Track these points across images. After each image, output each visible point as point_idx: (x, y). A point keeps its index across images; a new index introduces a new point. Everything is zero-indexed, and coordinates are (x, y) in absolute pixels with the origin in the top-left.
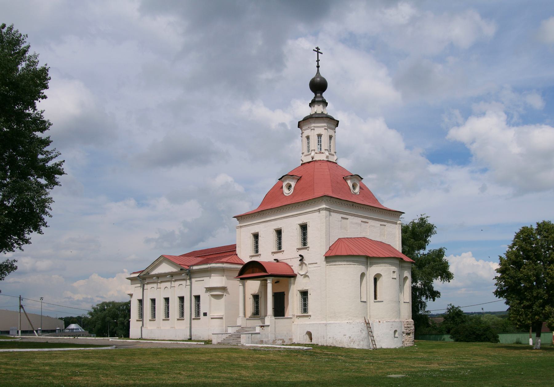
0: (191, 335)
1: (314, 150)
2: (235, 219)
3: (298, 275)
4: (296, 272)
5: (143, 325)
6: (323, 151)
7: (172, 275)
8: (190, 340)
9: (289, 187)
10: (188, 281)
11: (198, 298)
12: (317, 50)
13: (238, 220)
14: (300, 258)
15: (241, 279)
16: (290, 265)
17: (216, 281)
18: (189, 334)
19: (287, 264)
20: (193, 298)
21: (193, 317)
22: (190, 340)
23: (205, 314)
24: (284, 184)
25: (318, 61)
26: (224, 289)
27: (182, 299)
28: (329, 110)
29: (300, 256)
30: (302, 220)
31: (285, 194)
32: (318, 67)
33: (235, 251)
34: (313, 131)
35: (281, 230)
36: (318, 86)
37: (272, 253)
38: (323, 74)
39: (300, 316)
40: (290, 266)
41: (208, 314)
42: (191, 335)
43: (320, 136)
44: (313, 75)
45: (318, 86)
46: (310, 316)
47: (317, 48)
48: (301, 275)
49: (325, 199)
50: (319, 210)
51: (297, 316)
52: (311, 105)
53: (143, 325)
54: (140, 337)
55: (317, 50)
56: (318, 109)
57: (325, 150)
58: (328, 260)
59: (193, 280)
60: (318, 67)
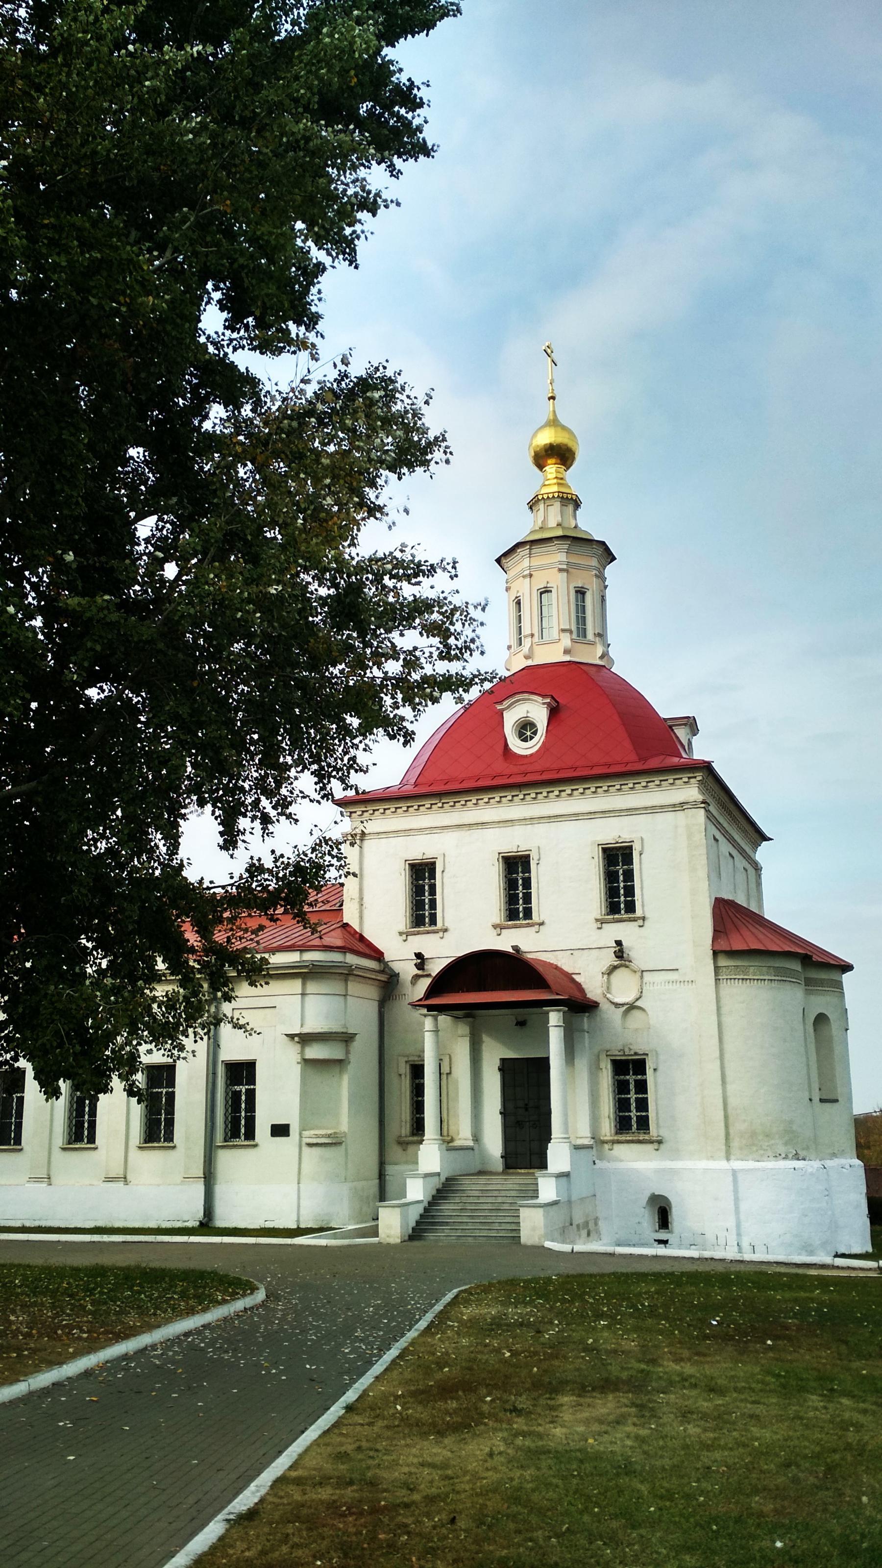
0: (209, 1210)
3: (604, 1006)
6: (590, 636)
9: (526, 729)
11: (242, 1072)
15: (430, 1008)
19: (557, 968)
20: (221, 1071)
22: (206, 1226)
23: (280, 1130)
24: (511, 718)
26: (346, 1038)
30: (613, 831)
33: (340, 910)
37: (495, 927)
42: (209, 1210)
43: (581, 593)
48: (617, 1005)
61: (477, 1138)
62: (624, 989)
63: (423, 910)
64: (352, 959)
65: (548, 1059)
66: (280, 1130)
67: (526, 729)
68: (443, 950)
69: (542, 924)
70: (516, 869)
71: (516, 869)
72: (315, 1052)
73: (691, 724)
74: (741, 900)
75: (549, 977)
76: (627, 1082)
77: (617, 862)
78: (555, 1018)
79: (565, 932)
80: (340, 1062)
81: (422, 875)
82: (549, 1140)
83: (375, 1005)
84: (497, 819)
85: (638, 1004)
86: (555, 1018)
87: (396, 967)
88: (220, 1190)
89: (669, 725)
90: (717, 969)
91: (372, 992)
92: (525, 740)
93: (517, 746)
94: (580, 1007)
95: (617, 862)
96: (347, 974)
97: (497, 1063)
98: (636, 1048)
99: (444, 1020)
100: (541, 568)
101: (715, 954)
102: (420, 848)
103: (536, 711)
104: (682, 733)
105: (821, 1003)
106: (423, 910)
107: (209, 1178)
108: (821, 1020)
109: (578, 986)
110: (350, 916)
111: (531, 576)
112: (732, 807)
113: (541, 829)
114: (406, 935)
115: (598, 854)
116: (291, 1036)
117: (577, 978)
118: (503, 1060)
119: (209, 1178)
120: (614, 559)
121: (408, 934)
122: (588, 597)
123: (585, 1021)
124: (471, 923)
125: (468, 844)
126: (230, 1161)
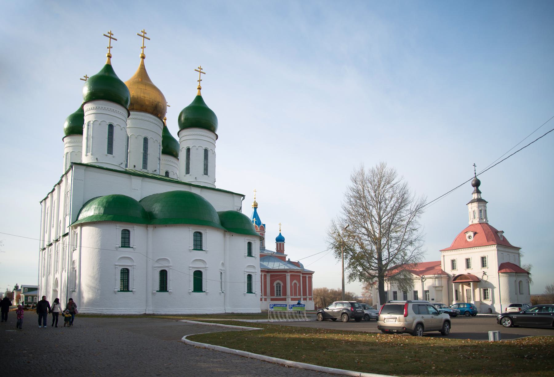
23: (433, 300)
28: (483, 196)
63: (453, 267)
66: (433, 300)
67: (469, 237)
68: (457, 273)
70: (468, 261)
71: (468, 261)
72: (437, 289)
73: (503, 232)
74: (512, 262)
77: (483, 260)
78: (471, 283)
79: (476, 270)
81: (453, 262)
93: (468, 240)
95: (483, 260)
103: (472, 234)
106: (453, 267)
125: (460, 256)
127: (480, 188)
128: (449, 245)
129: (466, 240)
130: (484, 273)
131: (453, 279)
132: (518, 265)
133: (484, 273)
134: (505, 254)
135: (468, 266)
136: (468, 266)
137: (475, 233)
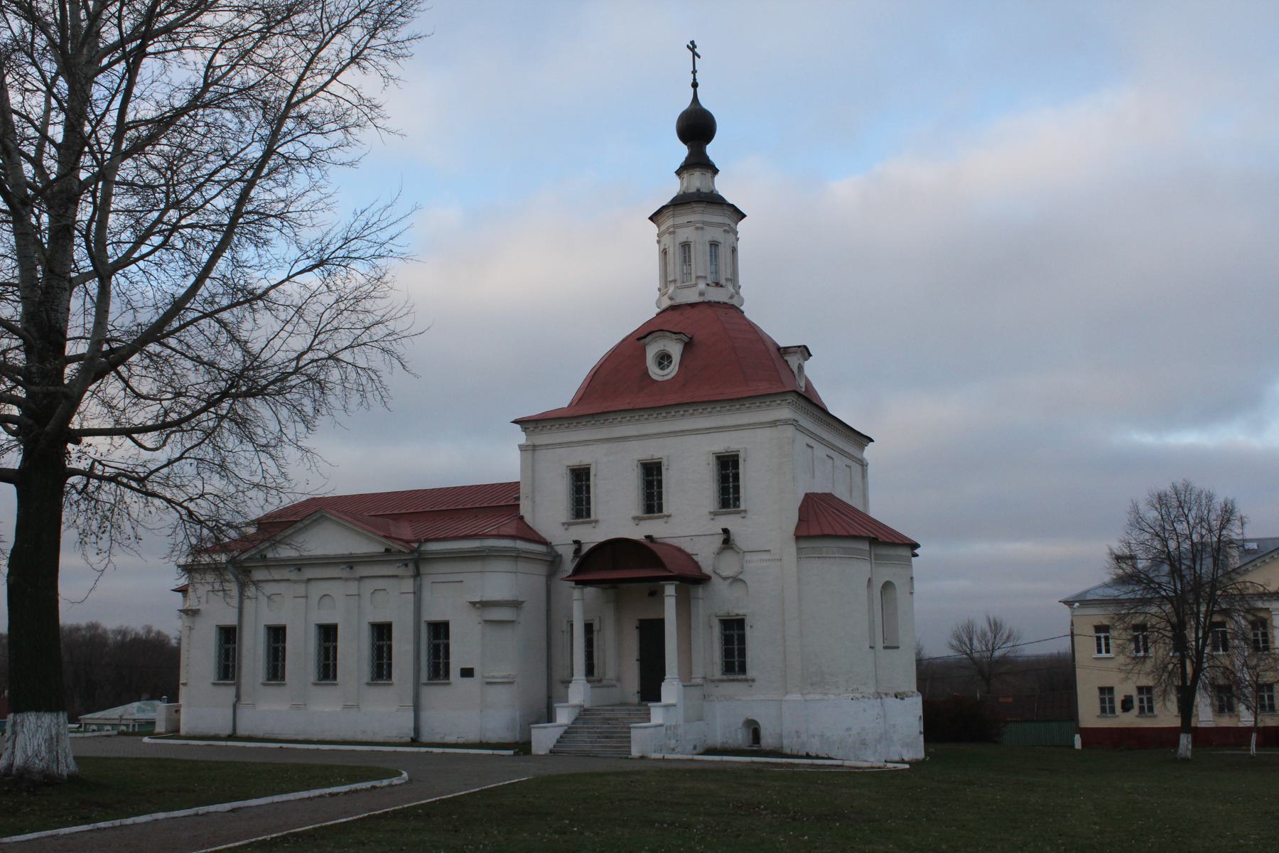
0: (417, 729)
1: (705, 277)
2: (518, 427)
3: (715, 579)
4: (707, 569)
5: (238, 696)
7: (350, 562)
8: (415, 742)
9: (664, 359)
10: (408, 585)
11: (440, 630)
12: (692, 47)
13: (525, 430)
14: (721, 538)
15: (578, 583)
16: (689, 550)
17: (499, 582)
18: (412, 725)
19: (680, 550)
20: (424, 629)
21: (424, 677)
22: (415, 742)
23: (468, 673)
24: (652, 352)
25: (694, 72)
26: (516, 605)
27: (382, 632)
29: (726, 531)
30: (723, 443)
31: (654, 377)
32: (695, 85)
34: (700, 232)
35: (660, 463)
36: (697, 128)
37: (634, 518)
38: (705, 103)
39: (722, 681)
40: (689, 556)
41: (476, 673)
42: (417, 729)
44: (685, 104)
45: (697, 128)
46: (753, 680)
47: (692, 43)
48: (725, 579)
49: (791, 398)
50: (774, 424)
51: (713, 681)
52: (679, 173)
53: (238, 696)
54: (228, 731)
55: (692, 47)
56: (696, 181)
57: (727, 280)
58: (804, 544)
59: (426, 582)
60: (695, 85)
61: (619, 679)
62: (728, 565)
63: (581, 506)
64: (521, 545)
65: (662, 621)
66: (468, 673)
67: (664, 359)
68: (592, 536)
69: (669, 516)
70: (652, 473)
71: (652, 473)
73: (805, 352)
74: (841, 493)
75: (666, 560)
76: (732, 636)
77: (728, 467)
78: (670, 589)
79: (688, 522)
80: (512, 622)
81: (580, 478)
82: (662, 679)
83: (543, 580)
84: (636, 433)
85: (741, 577)
86: (670, 589)
87: (560, 550)
88: (424, 715)
89: (784, 351)
90: (799, 549)
91: (541, 570)
92: (662, 369)
93: (655, 372)
94: (692, 579)
95: (728, 467)
96: (517, 556)
97: (636, 623)
98: (741, 612)
99: (590, 591)
100: (681, 226)
101: (798, 537)
102: (579, 457)
104: (793, 361)
105: (886, 573)
106: (581, 506)
107: (417, 709)
108: (888, 586)
109: (696, 563)
110: (525, 510)
111: (674, 232)
112: (830, 420)
113: (670, 441)
114: (567, 525)
115: (712, 461)
116: (473, 604)
117: (695, 558)
118: (641, 621)
119: (417, 709)
120: (744, 216)
121: (569, 524)
122: (721, 248)
123: (700, 591)
124: (618, 515)
126: (434, 695)
127: (712, 150)
128: (562, 396)
129: (646, 373)
130: (727, 540)
131: (569, 566)
132: (861, 508)
133: (727, 540)
134: (821, 451)
135: (652, 501)
136: (652, 501)
137: (688, 346)
